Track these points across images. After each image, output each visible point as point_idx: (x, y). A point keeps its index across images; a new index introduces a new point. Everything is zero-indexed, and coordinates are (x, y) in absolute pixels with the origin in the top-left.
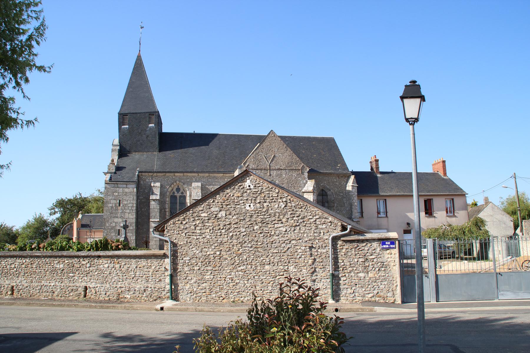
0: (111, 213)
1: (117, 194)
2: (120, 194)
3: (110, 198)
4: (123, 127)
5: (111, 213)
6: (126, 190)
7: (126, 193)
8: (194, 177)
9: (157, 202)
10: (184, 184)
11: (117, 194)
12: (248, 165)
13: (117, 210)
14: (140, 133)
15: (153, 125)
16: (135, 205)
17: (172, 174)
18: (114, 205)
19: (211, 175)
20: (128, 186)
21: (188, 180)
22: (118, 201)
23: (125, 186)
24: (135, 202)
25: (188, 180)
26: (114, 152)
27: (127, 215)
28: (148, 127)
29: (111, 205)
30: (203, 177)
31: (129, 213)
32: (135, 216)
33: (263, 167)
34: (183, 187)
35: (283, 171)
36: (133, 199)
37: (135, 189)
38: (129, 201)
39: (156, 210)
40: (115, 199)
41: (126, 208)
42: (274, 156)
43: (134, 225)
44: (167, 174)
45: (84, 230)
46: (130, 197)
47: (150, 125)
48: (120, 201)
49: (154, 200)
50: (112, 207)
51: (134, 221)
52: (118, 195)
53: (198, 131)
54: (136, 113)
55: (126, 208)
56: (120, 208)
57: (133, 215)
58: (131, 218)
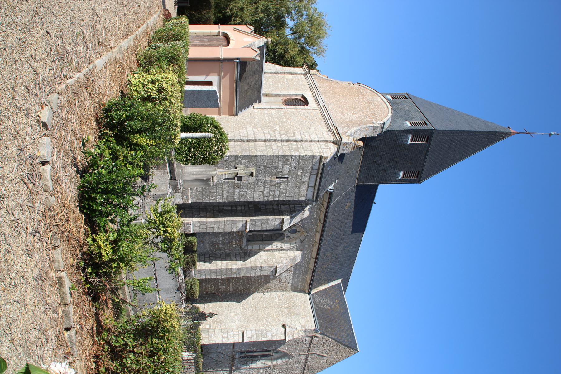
0: (265, 167)
1: (299, 173)
2: (299, 179)
3: (294, 165)
4: (411, 136)
5: (265, 167)
6: (304, 187)
7: (300, 187)
8: (311, 252)
9: (279, 227)
10: (302, 241)
11: (299, 173)
12: (317, 337)
13: (271, 175)
14: (393, 160)
15: (400, 177)
16: (276, 199)
17: (320, 229)
18: (280, 170)
19: (310, 272)
20: (311, 190)
21: (306, 246)
22: (286, 176)
23: (312, 184)
24: (281, 199)
25: (306, 246)
26: (372, 131)
27: (261, 189)
28: (400, 171)
29: (280, 166)
30: (309, 262)
31: (263, 192)
32: (257, 199)
33: (312, 348)
34: (296, 238)
35: (303, 364)
36: (286, 197)
37: (304, 199)
38: (283, 191)
39: (265, 226)
40: (290, 171)
41: (273, 188)
42: (324, 356)
43: (242, 200)
44: (320, 225)
45: (235, 69)
46: (290, 192)
47: (401, 174)
48: (288, 178)
49: (282, 222)
50: (277, 167)
51: (249, 199)
52: (297, 175)
53: (374, 207)
54: (426, 154)
55: (273, 188)
56: (274, 179)
57: (259, 197)
58: (257, 195)
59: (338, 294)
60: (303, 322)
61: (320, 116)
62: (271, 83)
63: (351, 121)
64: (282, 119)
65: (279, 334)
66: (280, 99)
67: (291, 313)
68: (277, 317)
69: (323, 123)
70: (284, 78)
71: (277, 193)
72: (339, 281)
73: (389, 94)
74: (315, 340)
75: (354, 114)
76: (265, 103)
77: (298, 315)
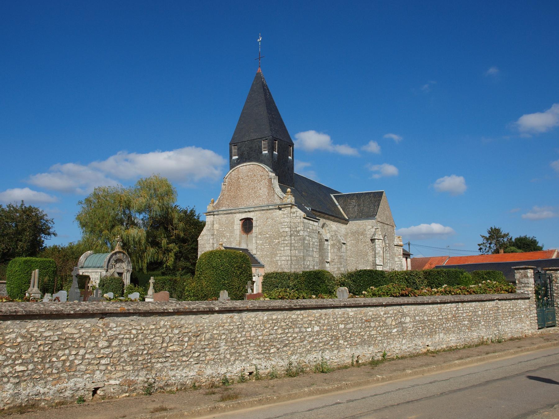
59: (344, 199)
60: (370, 227)
61: (263, 212)
62: (225, 240)
63: (268, 193)
64: (267, 237)
65: (378, 243)
66: (245, 236)
67: (362, 234)
68: (365, 243)
69: (272, 211)
70: (217, 230)
71: (316, 244)
72: (332, 195)
73: (231, 157)
74: (379, 219)
75: (260, 189)
76: (247, 246)
77: (365, 230)
